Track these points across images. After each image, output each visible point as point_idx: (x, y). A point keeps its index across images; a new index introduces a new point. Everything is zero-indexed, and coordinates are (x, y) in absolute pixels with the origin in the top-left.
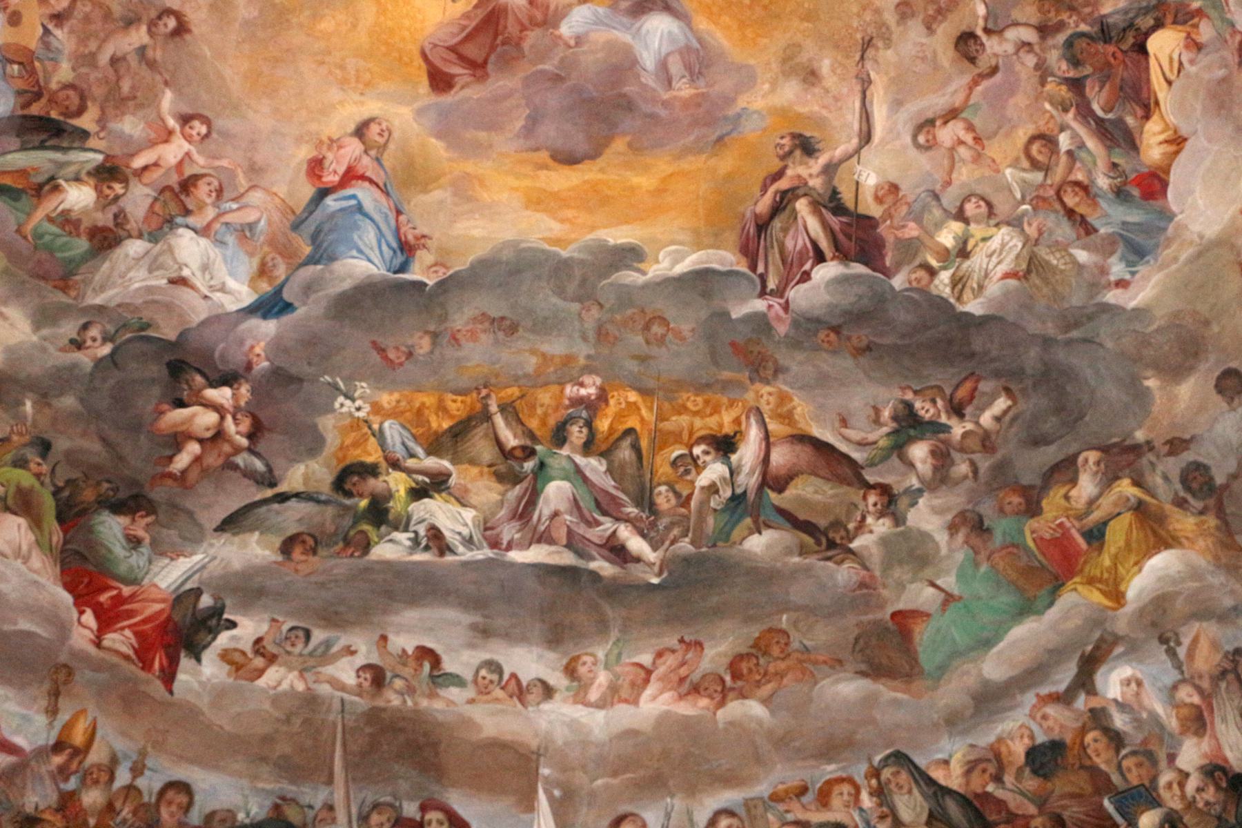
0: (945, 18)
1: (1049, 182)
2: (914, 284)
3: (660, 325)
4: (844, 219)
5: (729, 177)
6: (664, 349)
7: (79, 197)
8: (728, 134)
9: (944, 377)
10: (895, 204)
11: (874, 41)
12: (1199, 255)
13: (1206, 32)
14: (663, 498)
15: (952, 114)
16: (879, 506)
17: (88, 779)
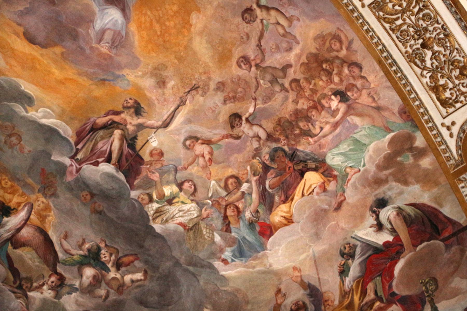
0: (234, 102)
1: (226, 198)
2: (140, 200)
3: (17, 139)
4: (130, 151)
5: (96, 99)
6: (10, 150)
8: (109, 80)
10: (157, 161)
11: (199, 89)
12: (265, 272)
13: (332, 186)
15: (208, 142)
16: (54, 284)
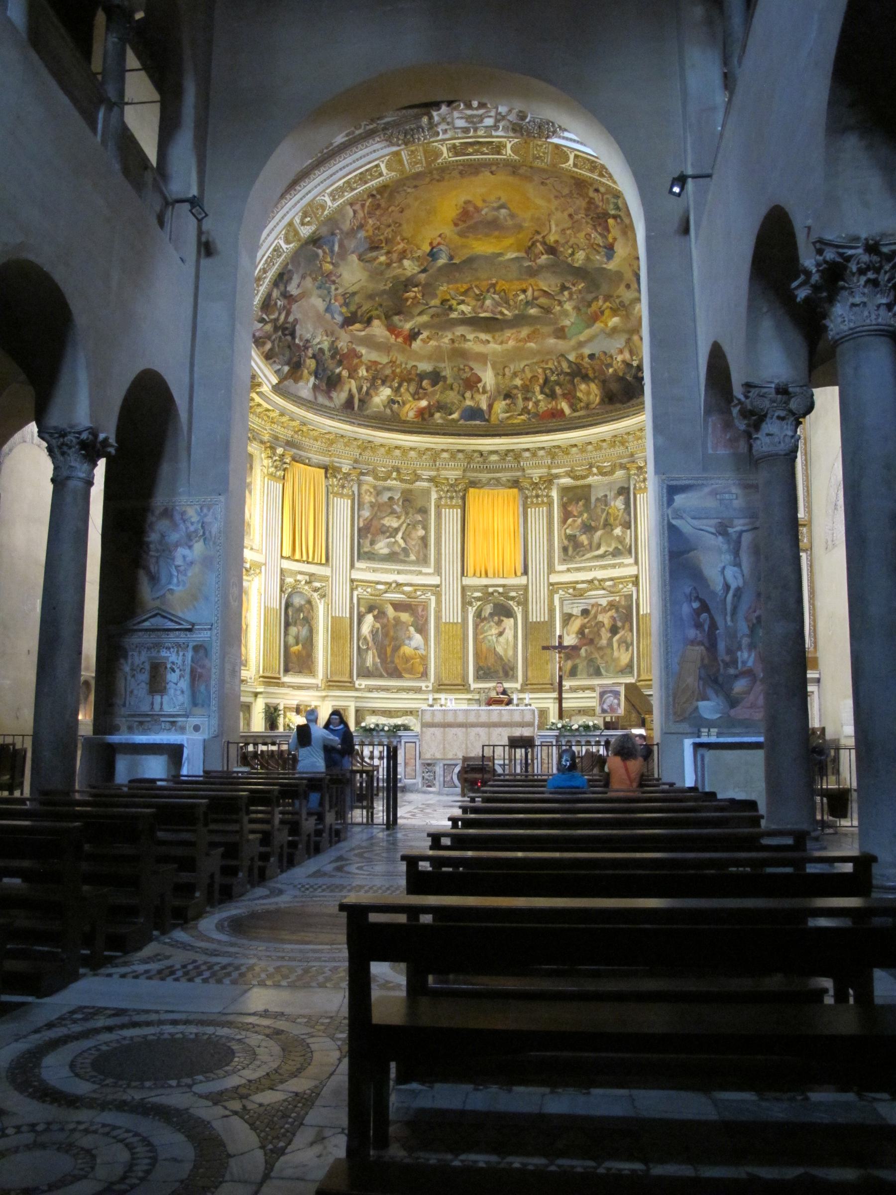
7: (383, 259)
9: (570, 278)
14: (511, 302)
15: (568, 229)
17: (397, 367)
